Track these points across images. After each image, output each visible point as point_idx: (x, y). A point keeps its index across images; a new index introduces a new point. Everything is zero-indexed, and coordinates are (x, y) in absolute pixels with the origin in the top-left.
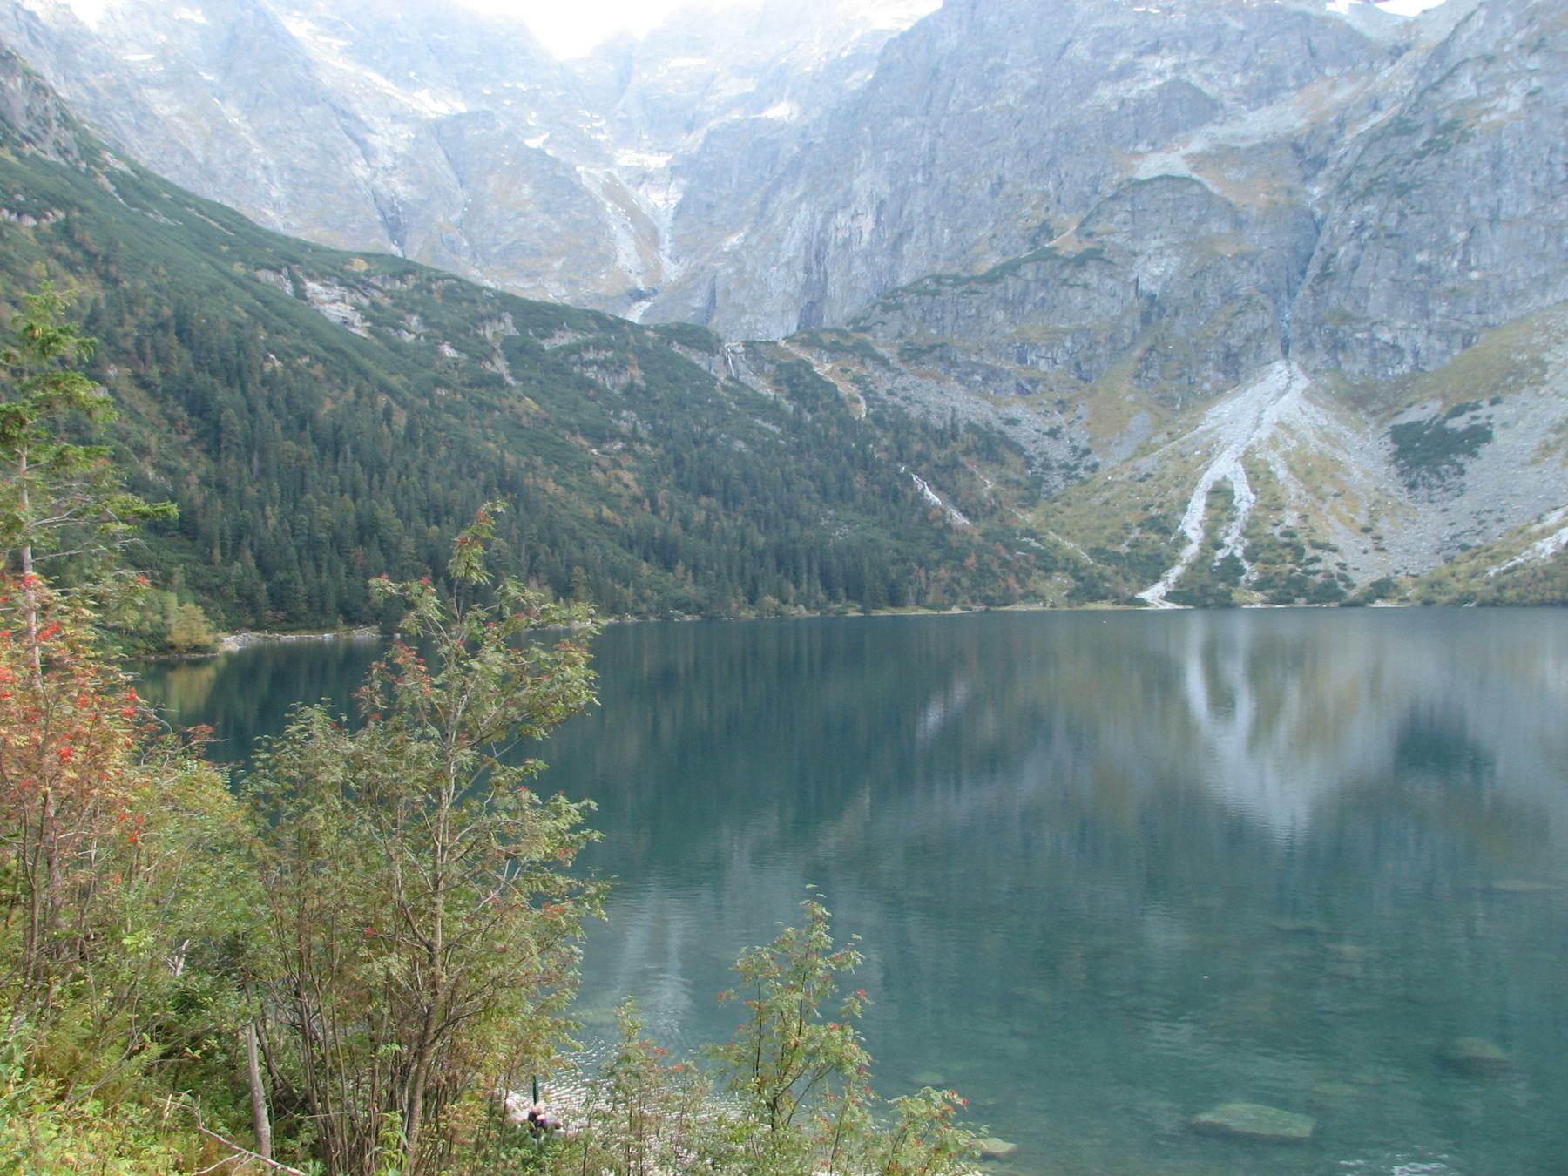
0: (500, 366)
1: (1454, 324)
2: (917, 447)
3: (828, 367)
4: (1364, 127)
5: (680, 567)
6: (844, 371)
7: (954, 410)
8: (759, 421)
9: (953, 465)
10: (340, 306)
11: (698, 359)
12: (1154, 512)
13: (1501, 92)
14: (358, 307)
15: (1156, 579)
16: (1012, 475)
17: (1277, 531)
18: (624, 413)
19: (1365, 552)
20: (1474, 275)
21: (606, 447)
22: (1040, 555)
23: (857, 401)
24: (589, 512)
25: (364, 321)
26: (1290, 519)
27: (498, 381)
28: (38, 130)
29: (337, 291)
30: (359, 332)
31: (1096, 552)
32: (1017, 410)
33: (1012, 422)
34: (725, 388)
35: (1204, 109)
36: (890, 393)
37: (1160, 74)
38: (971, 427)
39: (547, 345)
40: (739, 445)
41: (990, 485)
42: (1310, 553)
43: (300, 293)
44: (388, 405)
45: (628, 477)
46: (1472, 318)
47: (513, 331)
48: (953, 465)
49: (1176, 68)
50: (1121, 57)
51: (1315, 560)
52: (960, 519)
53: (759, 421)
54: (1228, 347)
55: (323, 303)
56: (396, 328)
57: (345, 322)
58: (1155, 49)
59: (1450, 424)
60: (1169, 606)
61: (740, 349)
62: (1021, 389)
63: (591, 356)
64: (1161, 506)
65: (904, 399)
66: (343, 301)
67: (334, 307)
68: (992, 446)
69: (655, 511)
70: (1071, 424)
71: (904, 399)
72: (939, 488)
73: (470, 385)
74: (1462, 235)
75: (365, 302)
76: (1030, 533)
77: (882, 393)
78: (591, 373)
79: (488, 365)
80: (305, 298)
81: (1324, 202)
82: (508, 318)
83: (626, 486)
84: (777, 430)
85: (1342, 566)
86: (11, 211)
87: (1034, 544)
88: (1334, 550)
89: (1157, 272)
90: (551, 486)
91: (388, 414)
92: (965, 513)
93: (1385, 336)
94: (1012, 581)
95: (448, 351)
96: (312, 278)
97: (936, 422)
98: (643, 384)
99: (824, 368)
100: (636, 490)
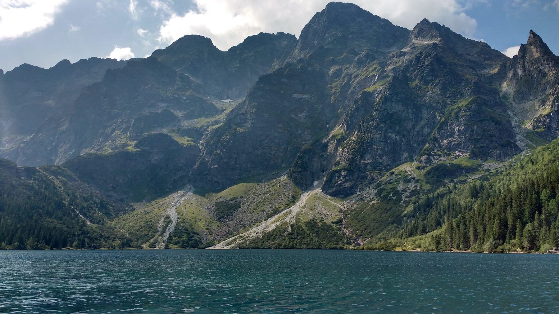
1: (232, 178)
2: (78, 201)
4: (214, 127)
7: (92, 193)
9: (90, 208)
12: (149, 223)
13: (247, 122)
15: (147, 241)
17: (183, 228)
19: (206, 235)
20: (238, 166)
22: (113, 234)
26: (187, 225)
31: (131, 234)
35: (174, 118)
37: (162, 107)
42: (192, 234)
46: (237, 176)
48: (90, 208)
49: (166, 107)
50: (152, 101)
51: (193, 237)
54: (174, 179)
58: (163, 101)
59: (230, 202)
60: (150, 249)
62: (113, 187)
64: (151, 221)
70: (127, 198)
74: (236, 155)
76: (110, 228)
81: (202, 145)
85: (200, 239)
88: (198, 234)
89: (156, 158)
92: (91, 222)
93: (216, 179)
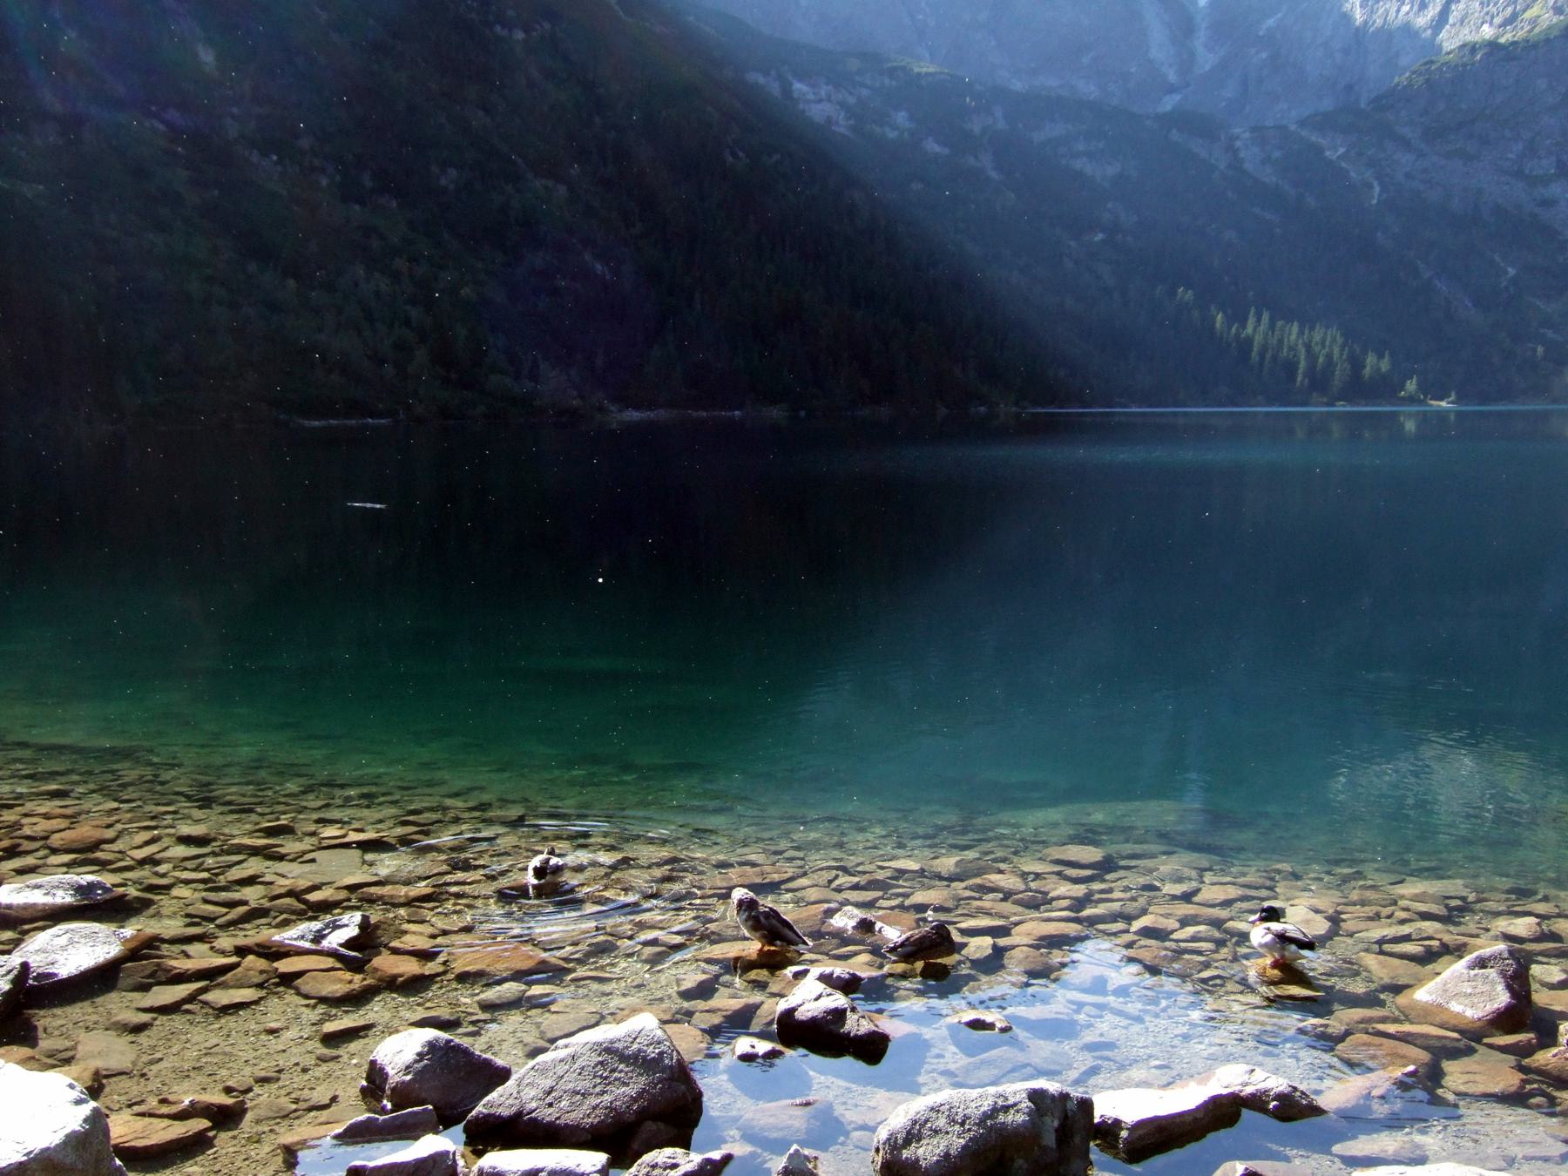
3: (1342, 150)
8: (1257, 210)
14: (842, 105)
23: (1371, 187)
25: (849, 119)
33: (1547, 203)
36: (1408, 176)
40: (1230, 235)
41: (1512, 271)
43: (787, 91)
53: (1257, 210)
55: (808, 102)
57: (829, 120)
61: (1247, 135)
63: (1081, 147)
66: (829, 100)
67: (820, 106)
75: (852, 100)
87: (1550, 334)
99: (1335, 149)
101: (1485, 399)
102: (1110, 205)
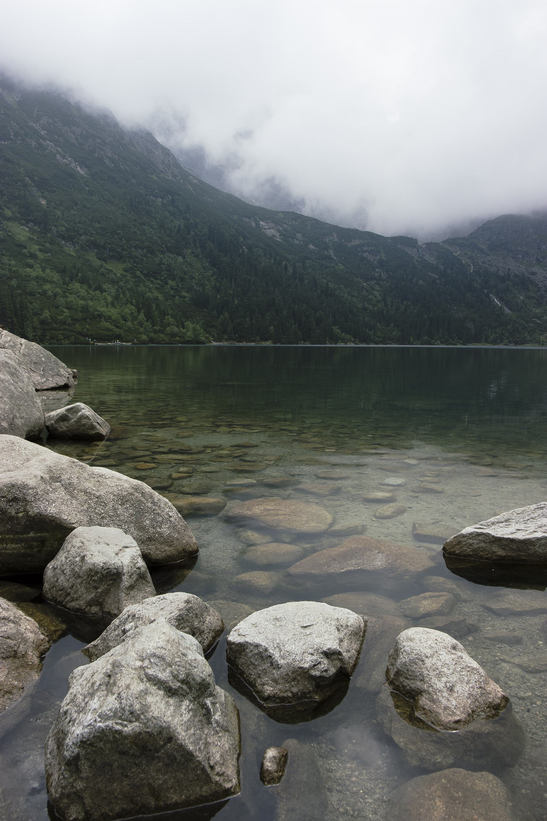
0: (331, 253)
3: (459, 253)
5: (392, 325)
6: (465, 254)
7: (509, 269)
10: (272, 231)
11: (408, 250)
14: (279, 231)
16: (531, 294)
18: (377, 270)
21: (369, 283)
23: (470, 266)
24: (360, 305)
27: (330, 258)
28: (166, 168)
29: (272, 225)
30: (278, 240)
32: (535, 269)
33: (534, 274)
34: (417, 261)
38: (516, 275)
39: (349, 245)
40: (421, 282)
41: (522, 298)
43: (258, 225)
44: (286, 264)
45: (377, 294)
47: (336, 240)
52: (507, 310)
53: (430, 274)
55: (266, 229)
56: (292, 238)
57: (274, 236)
62: (538, 260)
63: (366, 249)
65: (489, 265)
66: (273, 228)
68: (524, 283)
69: (386, 305)
71: (489, 265)
72: (501, 299)
73: (318, 259)
75: (281, 229)
77: (480, 263)
78: (365, 255)
79: (326, 252)
80: (260, 228)
82: (335, 236)
83: (375, 297)
84: (437, 277)
86: (154, 196)
90: (346, 296)
91: (286, 267)
92: (510, 309)
94: (526, 334)
95: (311, 247)
96: (262, 220)
97: (501, 273)
98: (385, 259)
99: (457, 253)
100: (380, 298)
101: (516, 343)
102: (377, 270)
